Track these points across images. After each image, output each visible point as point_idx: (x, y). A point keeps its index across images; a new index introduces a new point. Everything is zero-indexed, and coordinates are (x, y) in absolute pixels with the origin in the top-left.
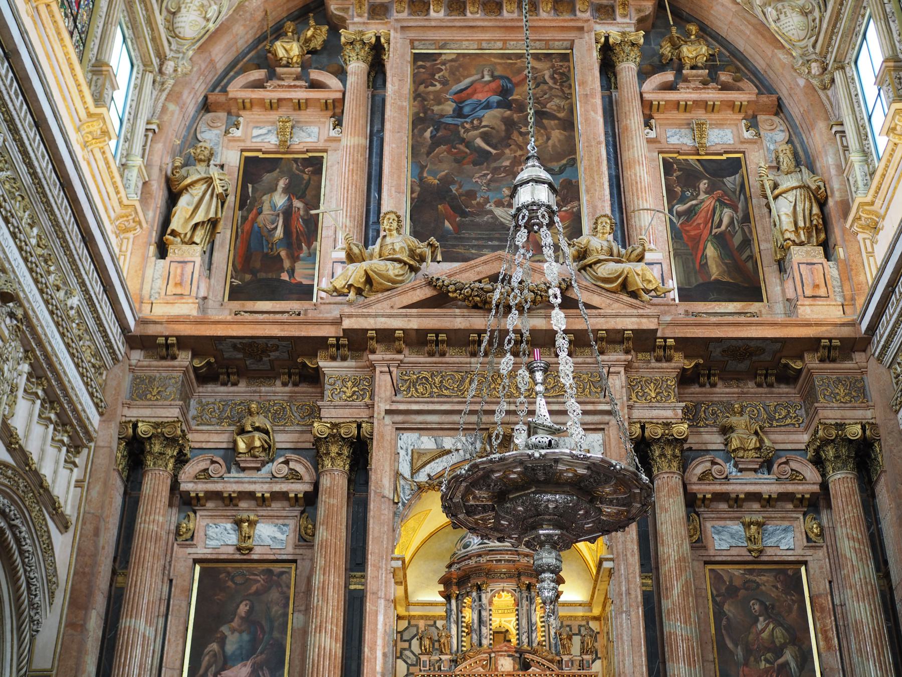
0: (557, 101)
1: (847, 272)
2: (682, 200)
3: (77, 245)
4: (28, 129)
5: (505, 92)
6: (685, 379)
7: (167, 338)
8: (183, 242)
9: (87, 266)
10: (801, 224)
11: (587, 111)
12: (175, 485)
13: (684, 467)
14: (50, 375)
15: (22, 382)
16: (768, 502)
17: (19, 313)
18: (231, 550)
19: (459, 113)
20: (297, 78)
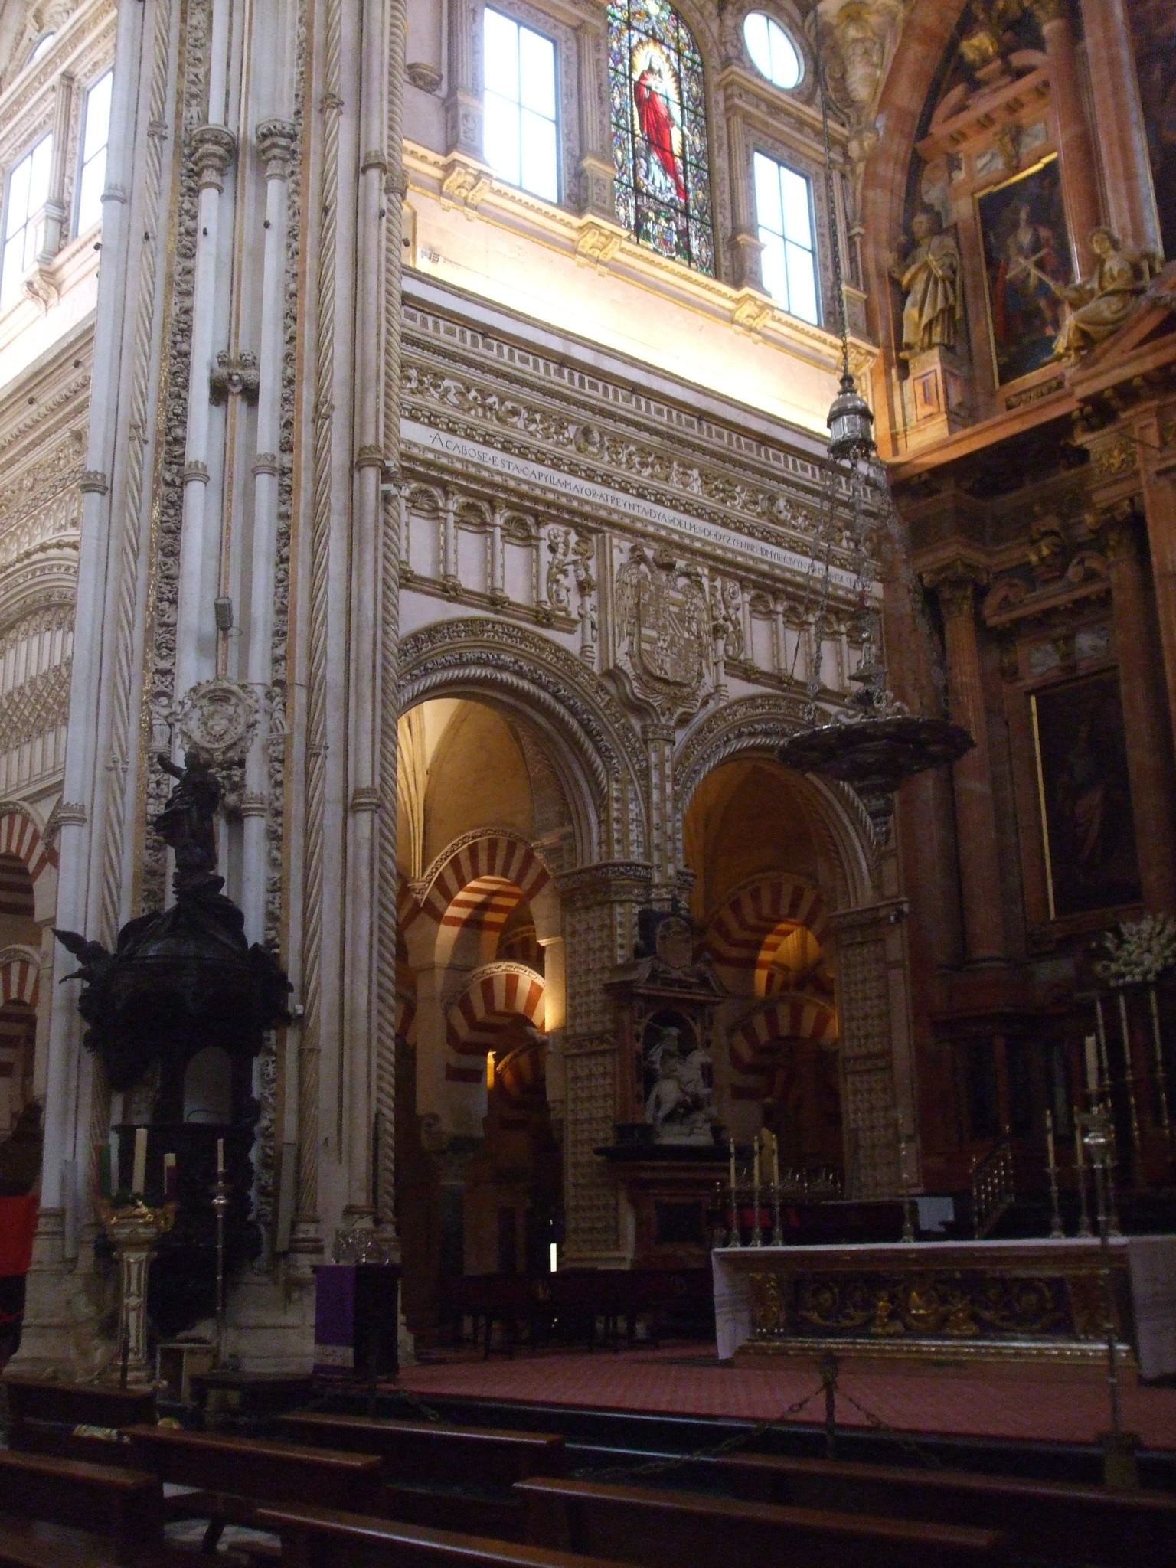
3: (754, 455)
4: (624, 405)
7: (919, 475)
8: (923, 350)
14: (779, 585)
15: (743, 615)
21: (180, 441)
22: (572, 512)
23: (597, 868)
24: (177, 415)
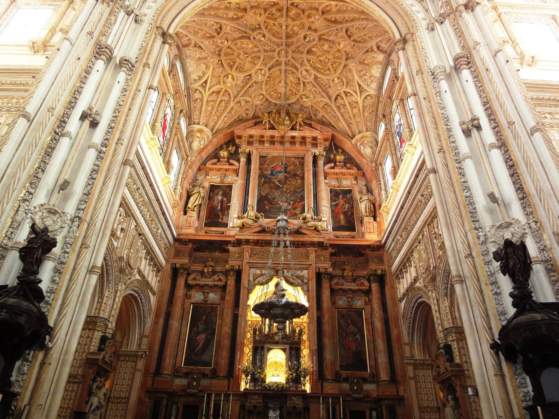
0: (300, 171)
1: (380, 225)
2: (335, 201)
5: (286, 168)
6: (332, 255)
9: (163, 221)
10: (367, 210)
11: (308, 175)
12: (186, 282)
13: (331, 280)
16: (354, 291)
17: (144, 238)
18: (201, 301)
19: (272, 174)
20: (226, 162)
21: (65, 122)
22: (128, 208)
23: (94, 317)
24: (67, 114)
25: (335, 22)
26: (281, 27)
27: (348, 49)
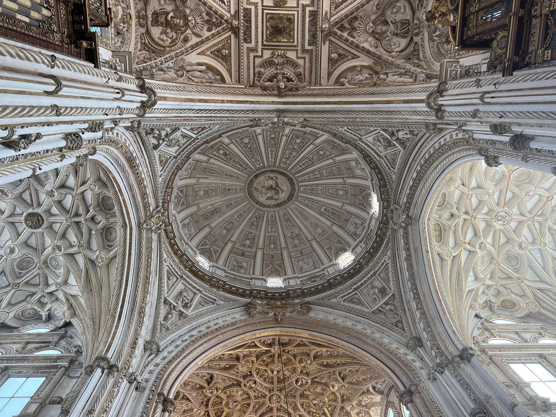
25: (328, 366)
26: (272, 372)
27: (342, 391)
